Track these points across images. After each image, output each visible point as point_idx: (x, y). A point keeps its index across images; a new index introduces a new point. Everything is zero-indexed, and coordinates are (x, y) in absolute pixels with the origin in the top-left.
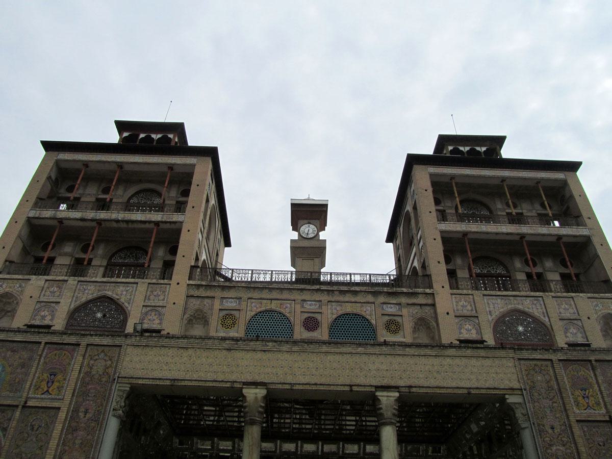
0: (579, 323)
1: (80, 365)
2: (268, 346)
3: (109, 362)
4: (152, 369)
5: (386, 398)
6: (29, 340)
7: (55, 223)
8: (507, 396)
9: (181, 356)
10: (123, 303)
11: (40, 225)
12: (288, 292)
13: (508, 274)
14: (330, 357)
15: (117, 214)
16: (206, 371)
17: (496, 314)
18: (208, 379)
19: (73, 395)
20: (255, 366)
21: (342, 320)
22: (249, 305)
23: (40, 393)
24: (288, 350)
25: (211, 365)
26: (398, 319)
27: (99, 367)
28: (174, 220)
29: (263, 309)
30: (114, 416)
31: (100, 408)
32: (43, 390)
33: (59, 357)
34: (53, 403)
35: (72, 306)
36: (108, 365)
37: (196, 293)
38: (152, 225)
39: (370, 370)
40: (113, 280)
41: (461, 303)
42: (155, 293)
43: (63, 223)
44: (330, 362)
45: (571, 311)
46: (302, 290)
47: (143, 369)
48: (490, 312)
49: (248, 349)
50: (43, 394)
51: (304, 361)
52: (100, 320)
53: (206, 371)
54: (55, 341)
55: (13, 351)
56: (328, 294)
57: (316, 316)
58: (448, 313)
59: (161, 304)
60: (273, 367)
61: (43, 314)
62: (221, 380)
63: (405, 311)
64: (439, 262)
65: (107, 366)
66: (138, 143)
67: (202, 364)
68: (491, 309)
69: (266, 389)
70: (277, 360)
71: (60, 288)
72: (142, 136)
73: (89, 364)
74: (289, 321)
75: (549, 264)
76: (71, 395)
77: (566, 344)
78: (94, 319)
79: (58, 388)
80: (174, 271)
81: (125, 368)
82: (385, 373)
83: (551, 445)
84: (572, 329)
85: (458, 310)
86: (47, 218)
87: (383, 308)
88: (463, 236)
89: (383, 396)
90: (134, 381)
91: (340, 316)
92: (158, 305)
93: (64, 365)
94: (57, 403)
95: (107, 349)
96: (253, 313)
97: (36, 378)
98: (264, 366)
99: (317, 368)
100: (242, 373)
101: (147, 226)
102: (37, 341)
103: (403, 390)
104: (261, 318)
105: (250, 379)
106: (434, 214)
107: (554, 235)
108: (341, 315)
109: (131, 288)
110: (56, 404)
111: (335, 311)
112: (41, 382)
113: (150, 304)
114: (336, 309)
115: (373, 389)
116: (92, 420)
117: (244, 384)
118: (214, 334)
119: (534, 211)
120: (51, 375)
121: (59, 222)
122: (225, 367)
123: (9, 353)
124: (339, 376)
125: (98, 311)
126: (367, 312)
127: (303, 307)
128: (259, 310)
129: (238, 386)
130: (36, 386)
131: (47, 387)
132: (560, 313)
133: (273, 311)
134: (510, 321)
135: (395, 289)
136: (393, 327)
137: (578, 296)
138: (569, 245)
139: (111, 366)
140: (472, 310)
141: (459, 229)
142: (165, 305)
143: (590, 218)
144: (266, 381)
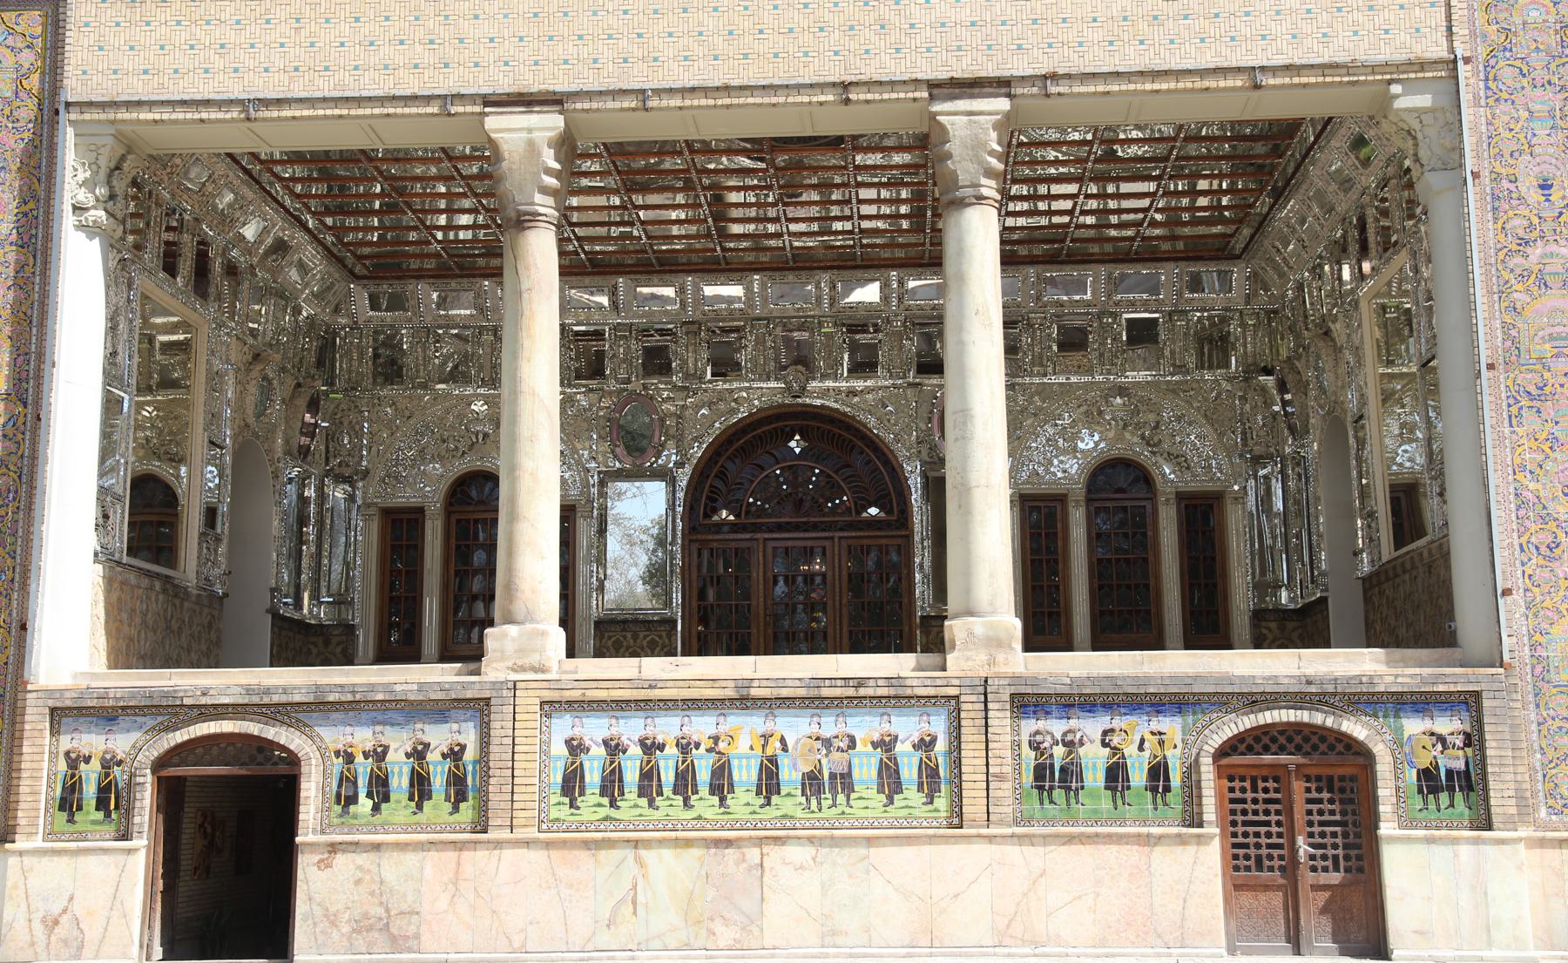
4: (176, 71)
9: (268, 22)
16: (356, 68)
18: (365, 93)
25: (372, 44)
30: (81, 227)
31: (31, 205)
36: (27, 65)
39: (912, 26)
47: (146, 72)
51: (685, 10)
53: (356, 68)
62: (408, 93)
65: (24, 71)
67: (342, 45)
69: (560, 113)
70: (595, 14)
81: (84, 73)
82: (965, 34)
98: (551, 38)
99: (731, 33)
100: (477, 65)
105: (504, 84)
122: (419, 48)
124: (806, 54)
144: (558, 88)
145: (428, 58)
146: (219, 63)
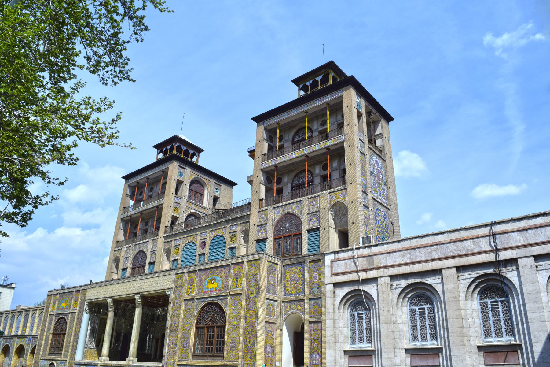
7: (129, 218)
17: (277, 218)
37: (167, 241)
38: (156, 208)
41: (262, 217)
45: (316, 206)
48: (274, 218)
55: (70, 295)
59: (155, 249)
63: (239, 228)
71: (129, 250)
83: (174, 311)
87: (230, 229)
90: (89, 301)
103: (141, 294)
107: (322, 149)
127: (201, 237)
137: (322, 193)
140: (266, 220)
141: (271, 164)
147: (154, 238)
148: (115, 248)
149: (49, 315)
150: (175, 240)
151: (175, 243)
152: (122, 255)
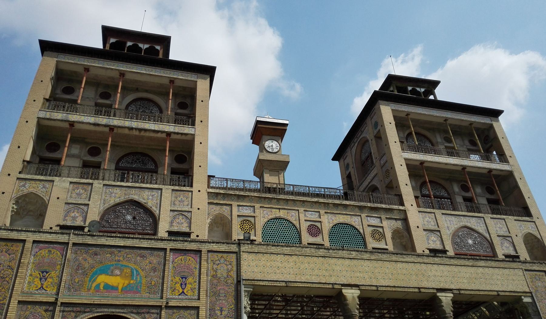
0: (510, 239)
1: (206, 269)
2: (352, 254)
3: (230, 267)
4: (268, 273)
5: (445, 298)
6: (155, 247)
7: (66, 125)
8: (523, 297)
9: (288, 262)
10: (151, 207)
11: (48, 126)
12: (293, 202)
13: (449, 197)
14: (400, 265)
15: (131, 122)
16: (310, 275)
19: (207, 296)
20: (347, 271)
21: (337, 228)
22: (261, 212)
23: (177, 294)
24: (368, 258)
25: (313, 269)
26: (381, 230)
27: (222, 271)
28: (186, 132)
29: (273, 216)
32: (179, 291)
33: (185, 262)
34: (192, 303)
35: (102, 208)
36: (230, 269)
38: (164, 135)
40: (137, 185)
42: (179, 199)
43: (74, 126)
44: (400, 269)
46: (304, 201)
47: (260, 272)
48: (448, 227)
49: (338, 257)
50: (180, 295)
52: (130, 222)
53: (310, 275)
54: (179, 248)
55: (142, 256)
56: (325, 206)
57: (317, 224)
58: (418, 227)
59: (187, 209)
60: (360, 272)
61: (73, 215)
62: (324, 282)
63: (385, 223)
64: (406, 185)
66: (126, 52)
67: (306, 269)
68: (449, 225)
69: (359, 289)
72: (129, 44)
73: (213, 269)
74: (296, 227)
75: (479, 190)
76: (205, 296)
77: (503, 255)
78: (125, 221)
79: (192, 289)
80: (194, 179)
81: (246, 272)
84: (506, 244)
85: (424, 225)
86: (59, 120)
87: (367, 220)
88: (420, 164)
89: (443, 296)
91: (335, 225)
92: (184, 209)
93: (191, 269)
94: (196, 303)
95: (225, 255)
96: (266, 220)
97: (170, 281)
98: (353, 271)
99: (392, 274)
100: (338, 276)
101: (159, 135)
102: (162, 247)
103: (455, 292)
104: (272, 224)
106: (398, 143)
108: (336, 224)
109: (156, 194)
110: (194, 303)
111: (331, 221)
112: (175, 285)
113: (177, 209)
114: (331, 219)
115: (435, 291)
116: (228, 317)
117: (343, 285)
118: (236, 236)
119: (465, 146)
120: (182, 278)
121: (69, 124)
122: (324, 271)
123: (139, 258)
124: (409, 280)
125: (128, 213)
126: (356, 223)
128: (271, 217)
129: (338, 287)
130: (171, 288)
131: (182, 288)
132: (497, 231)
133: (282, 219)
134: (463, 235)
135: (376, 204)
136: (377, 236)
137: (508, 218)
138: (497, 177)
139: (232, 270)
140: (435, 225)
142: (190, 210)
143: (511, 157)
144: (358, 284)
145: (327, 274)
146: (278, 271)
147: (177, 188)
148: (20, 173)
149: (14, 304)
150: (239, 206)
151: (239, 211)
152: (54, 195)
